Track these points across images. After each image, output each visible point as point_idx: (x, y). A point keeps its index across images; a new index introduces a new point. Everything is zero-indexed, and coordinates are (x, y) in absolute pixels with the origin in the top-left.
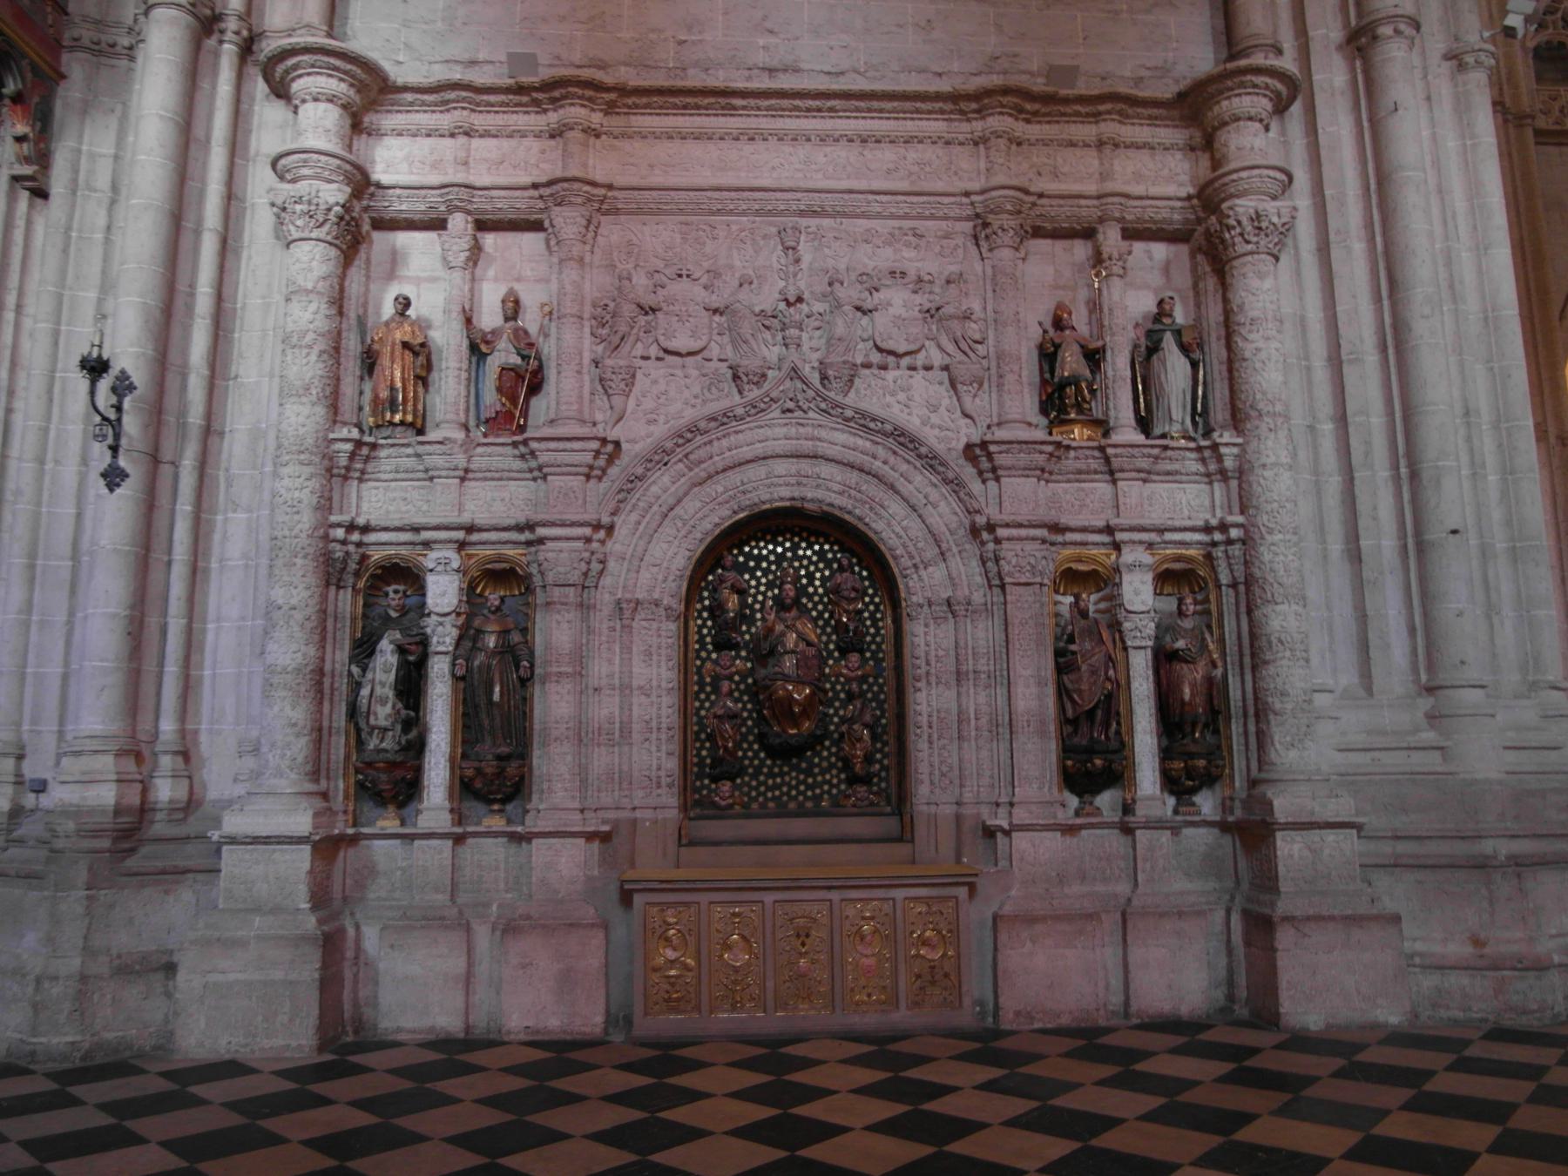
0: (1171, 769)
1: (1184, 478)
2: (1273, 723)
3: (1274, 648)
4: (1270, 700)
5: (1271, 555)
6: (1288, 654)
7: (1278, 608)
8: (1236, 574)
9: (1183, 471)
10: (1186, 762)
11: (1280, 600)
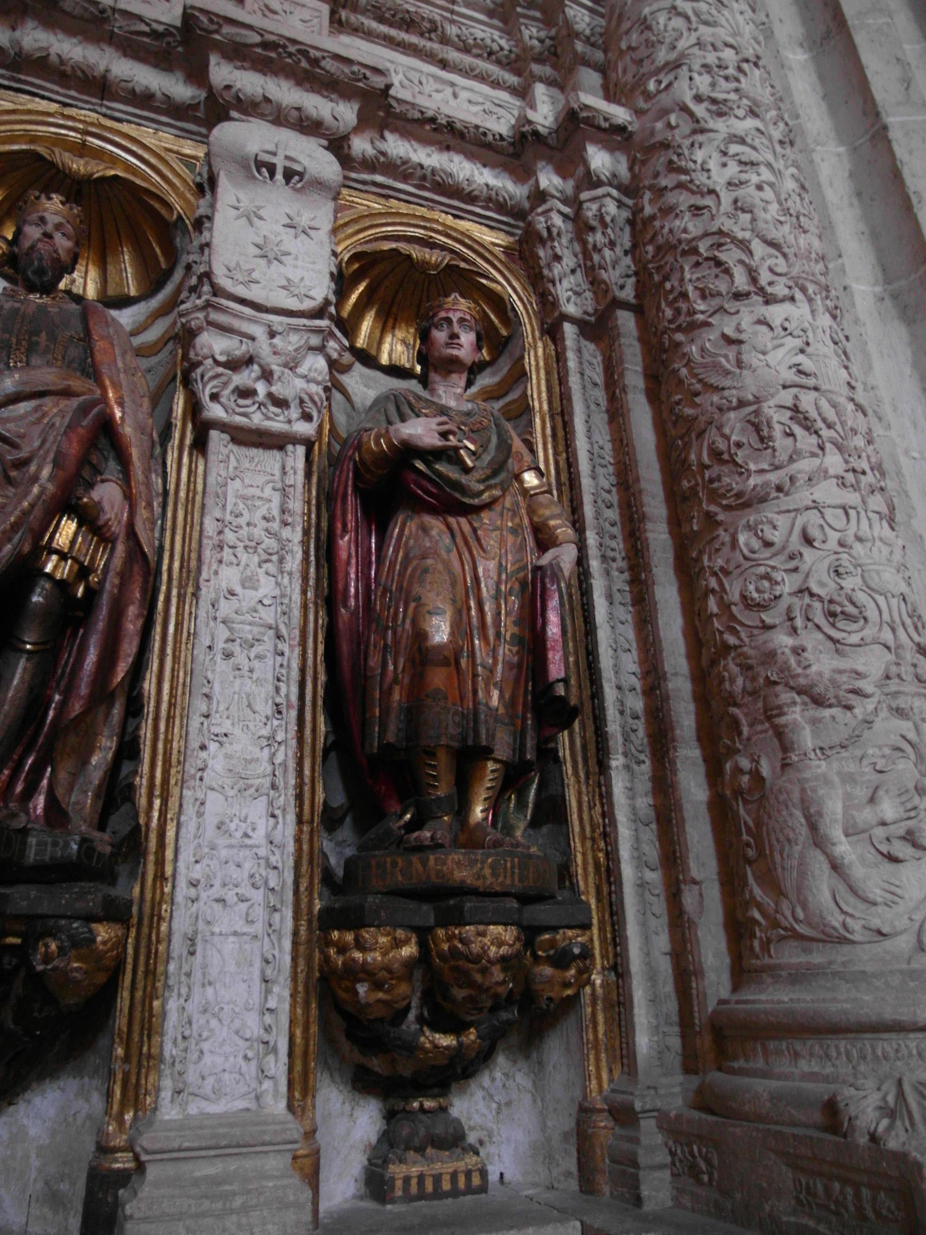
0: (355, 973)
1: (453, 55)
2: (807, 739)
3: (780, 442)
4: (783, 640)
5: (733, 169)
6: (833, 461)
7: (776, 313)
8: (611, 276)
9: (452, 31)
10: (423, 935)
11: (780, 290)
